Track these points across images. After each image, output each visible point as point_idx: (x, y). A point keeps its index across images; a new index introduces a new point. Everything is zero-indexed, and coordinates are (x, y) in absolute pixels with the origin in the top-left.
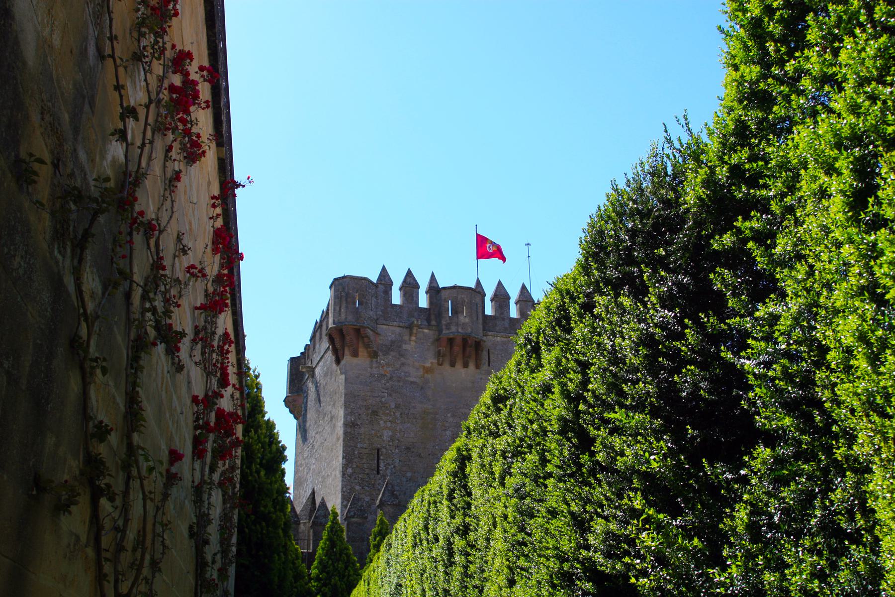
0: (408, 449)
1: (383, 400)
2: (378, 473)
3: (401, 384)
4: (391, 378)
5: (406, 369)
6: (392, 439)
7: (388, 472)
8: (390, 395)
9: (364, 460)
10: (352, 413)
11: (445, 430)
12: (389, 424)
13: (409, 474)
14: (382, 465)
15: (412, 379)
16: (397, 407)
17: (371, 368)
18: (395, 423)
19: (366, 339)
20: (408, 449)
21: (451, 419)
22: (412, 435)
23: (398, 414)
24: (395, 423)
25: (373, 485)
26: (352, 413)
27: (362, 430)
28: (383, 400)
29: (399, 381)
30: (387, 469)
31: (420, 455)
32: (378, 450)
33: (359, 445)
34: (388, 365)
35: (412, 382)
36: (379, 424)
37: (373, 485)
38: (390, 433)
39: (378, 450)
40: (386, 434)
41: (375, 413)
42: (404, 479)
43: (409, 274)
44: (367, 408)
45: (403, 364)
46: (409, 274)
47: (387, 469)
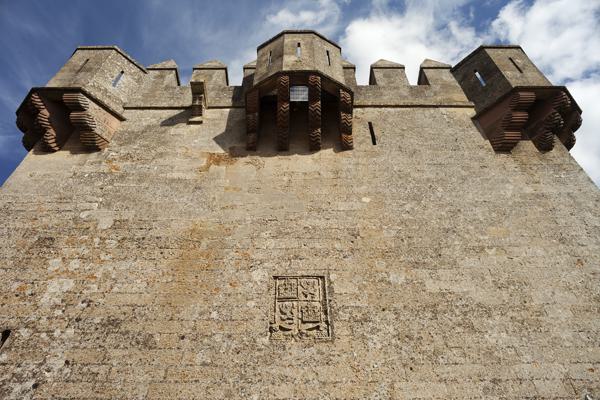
0: (112, 323)
1: (83, 215)
5: (167, 161)
6: (67, 302)
12: (74, 264)
15: (175, 175)
16: (118, 225)
22: (140, 284)
28: (83, 215)
31: (147, 343)
35: (173, 180)
41: (47, 242)
45: (161, 155)
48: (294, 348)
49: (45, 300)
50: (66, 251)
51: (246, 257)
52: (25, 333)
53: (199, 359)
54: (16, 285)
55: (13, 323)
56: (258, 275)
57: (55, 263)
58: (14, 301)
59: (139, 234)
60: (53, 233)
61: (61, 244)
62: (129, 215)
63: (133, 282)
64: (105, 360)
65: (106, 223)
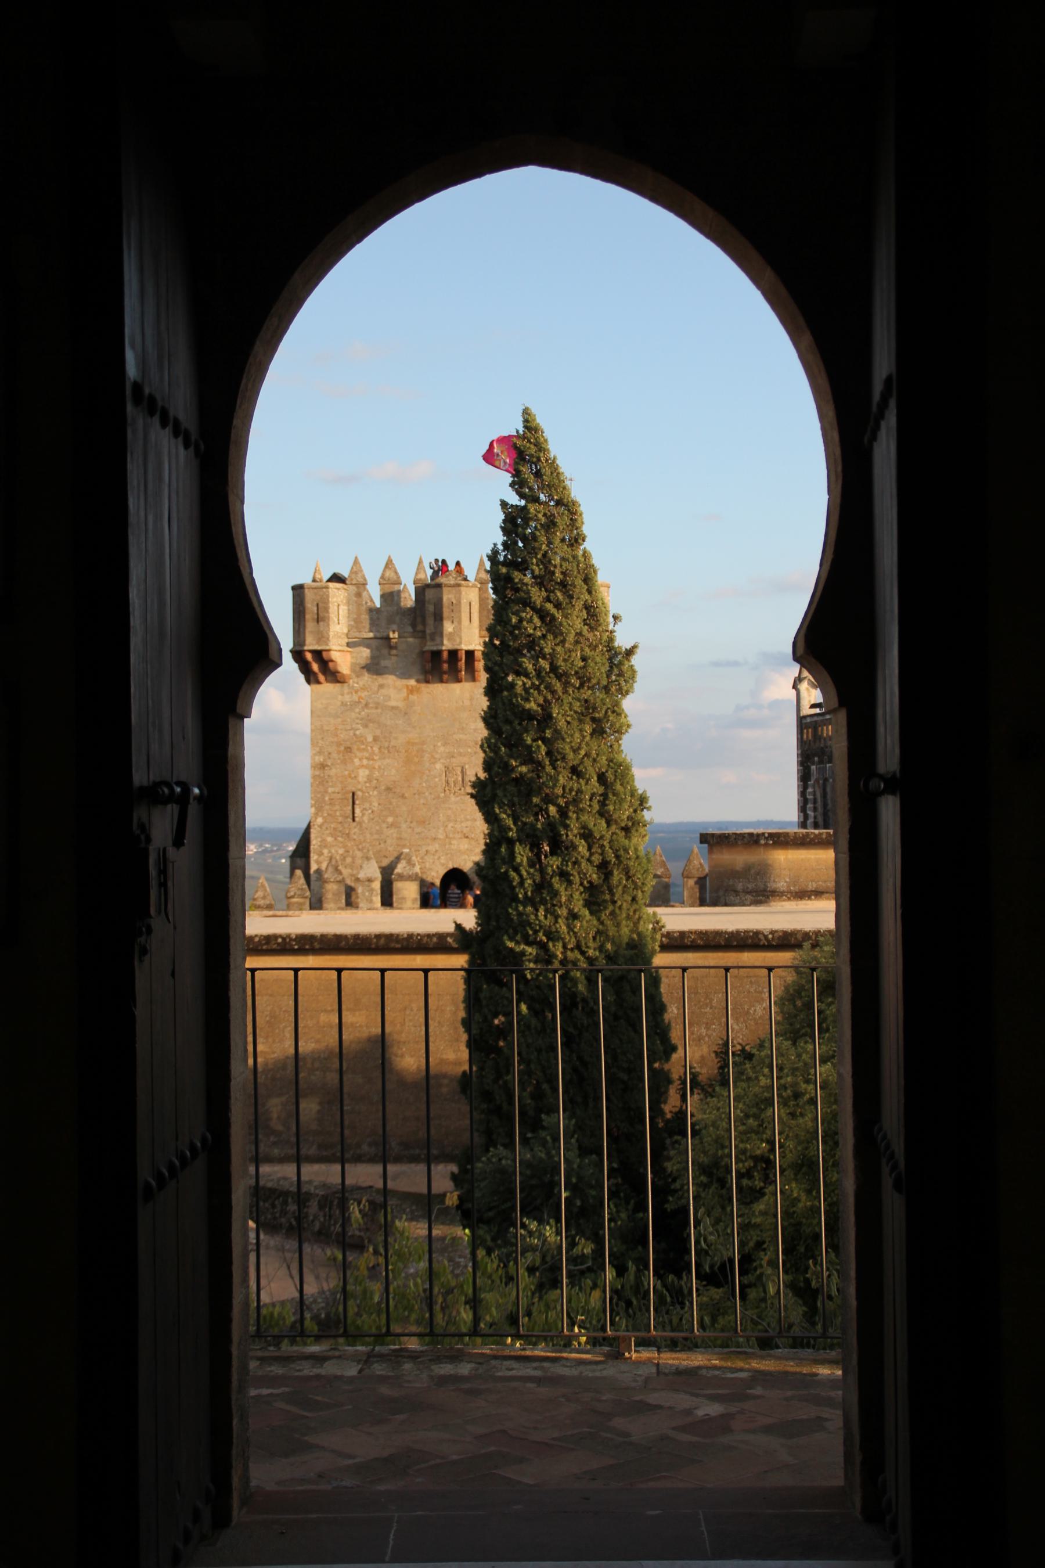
0: (388, 789)
1: (358, 732)
2: (354, 820)
3: (379, 711)
4: (367, 705)
5: (383, 691)
6: (369, 779)
7: (366, 819)
8: (366, 726)
9: (337, 807)
10: (320, 753)
11: (434, 763)
12: (365, 762)
13: (390, 820)
14: (358, 811)
15: (393, 703)
16: (376, 739)
17: (342, 695)
18: (373, 759)
19: (331, 665)
20: (388, 789)
21: (442, 749)
22: (393, 772)
23: (376, 749)
24: (373, 759)
25: (348, 835)
26: (320, 753)
27: (333, 772)
28: (358, 732)
29: (377, 708)
30: (363, 815)
31: (403, 796)
32: (353, 794)
33: (330, 790)
34: (363, 689)
36: (353, 762)
37: (348, 835)
38: (367, 772)
39: (353, 794)
40: (363, 774)
41: (348, 749)
42: (384, 825)
43: (389, 564)
44: (339, 744)
46: (389, 564)
47: (363, 815)
48: (453, 798)
49: (360, 779)
50: (359, 754)
51: (433, 757)
52: (359, 794)
53: (422, 801)
54: (346, 773)
55: (353, 789)
56: (438, 766)
57: (356, 761)
58: (350, 780)
59: (386, 745)
60: (348, 744)
61: (355, 750)
62: (378, 732)
63: (391, 769)
64: (391, 803)
65: (370, 739)
